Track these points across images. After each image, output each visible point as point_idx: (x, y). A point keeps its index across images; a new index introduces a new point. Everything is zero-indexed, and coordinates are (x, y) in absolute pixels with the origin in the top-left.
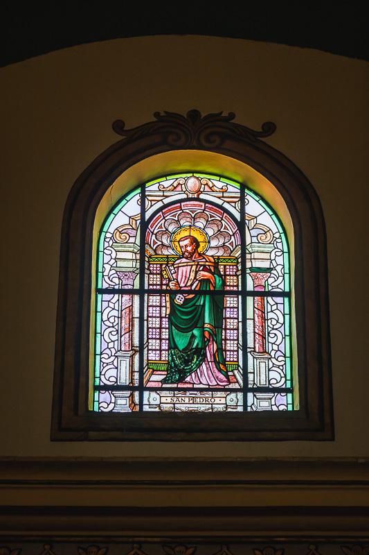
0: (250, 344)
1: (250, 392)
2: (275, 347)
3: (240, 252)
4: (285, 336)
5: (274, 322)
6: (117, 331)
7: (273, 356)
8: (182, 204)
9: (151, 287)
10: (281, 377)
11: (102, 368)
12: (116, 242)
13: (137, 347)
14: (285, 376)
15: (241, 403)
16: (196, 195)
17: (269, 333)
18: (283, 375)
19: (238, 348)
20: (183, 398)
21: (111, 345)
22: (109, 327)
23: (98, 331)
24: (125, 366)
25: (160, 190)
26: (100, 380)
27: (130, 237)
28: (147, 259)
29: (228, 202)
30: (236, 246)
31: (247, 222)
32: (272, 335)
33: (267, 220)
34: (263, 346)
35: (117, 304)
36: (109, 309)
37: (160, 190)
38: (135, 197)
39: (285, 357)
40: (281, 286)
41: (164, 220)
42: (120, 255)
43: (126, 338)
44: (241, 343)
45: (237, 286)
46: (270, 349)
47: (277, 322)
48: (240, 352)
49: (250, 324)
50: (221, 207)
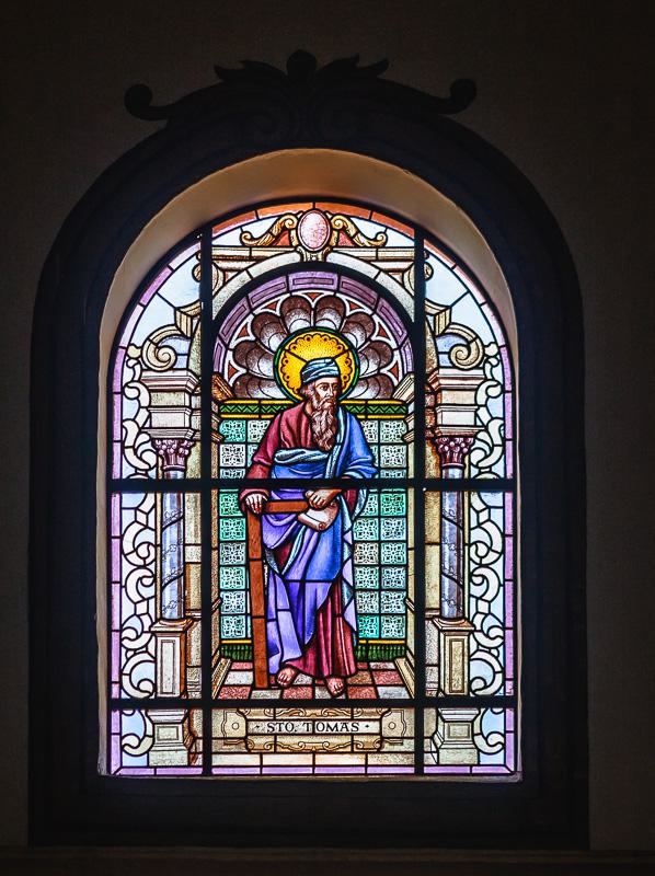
0: (432, 599)
1: (429, 706)
2: (483, 607)
3: (412, 389)
4: (505, 580)
5: (482, 550)
6: (154, 576)
7: (478, 628)
10: (495, 673)
11: (124, 660)
12: (149, 369)
13: (196, 610)
14: (503, 671)
15: (410, 732)
16: (320, 255)
17: (471, 574)
18: (498, 668)
19: (407, 607)
21: (142, 608)
22: (139, 567)
23: (116, 577)
24: (170, 652)
25: (244, 245)
26: (121, 687)
27: (177, 355)
28: (215, 408)
29: (387, 272)
30: (404, 376)
31: (430, 319)
32: (477, 580)
33: (471, 315)
34: (460, 605)
35: (152, 515)
36: (137, 527)
38: (187, 262)
39: (504, 628)
40: (499, 469)
43: (170, 594)
46: (473, 611)
47: (490, 549)
49: (432, 553)
50: (371, 283)
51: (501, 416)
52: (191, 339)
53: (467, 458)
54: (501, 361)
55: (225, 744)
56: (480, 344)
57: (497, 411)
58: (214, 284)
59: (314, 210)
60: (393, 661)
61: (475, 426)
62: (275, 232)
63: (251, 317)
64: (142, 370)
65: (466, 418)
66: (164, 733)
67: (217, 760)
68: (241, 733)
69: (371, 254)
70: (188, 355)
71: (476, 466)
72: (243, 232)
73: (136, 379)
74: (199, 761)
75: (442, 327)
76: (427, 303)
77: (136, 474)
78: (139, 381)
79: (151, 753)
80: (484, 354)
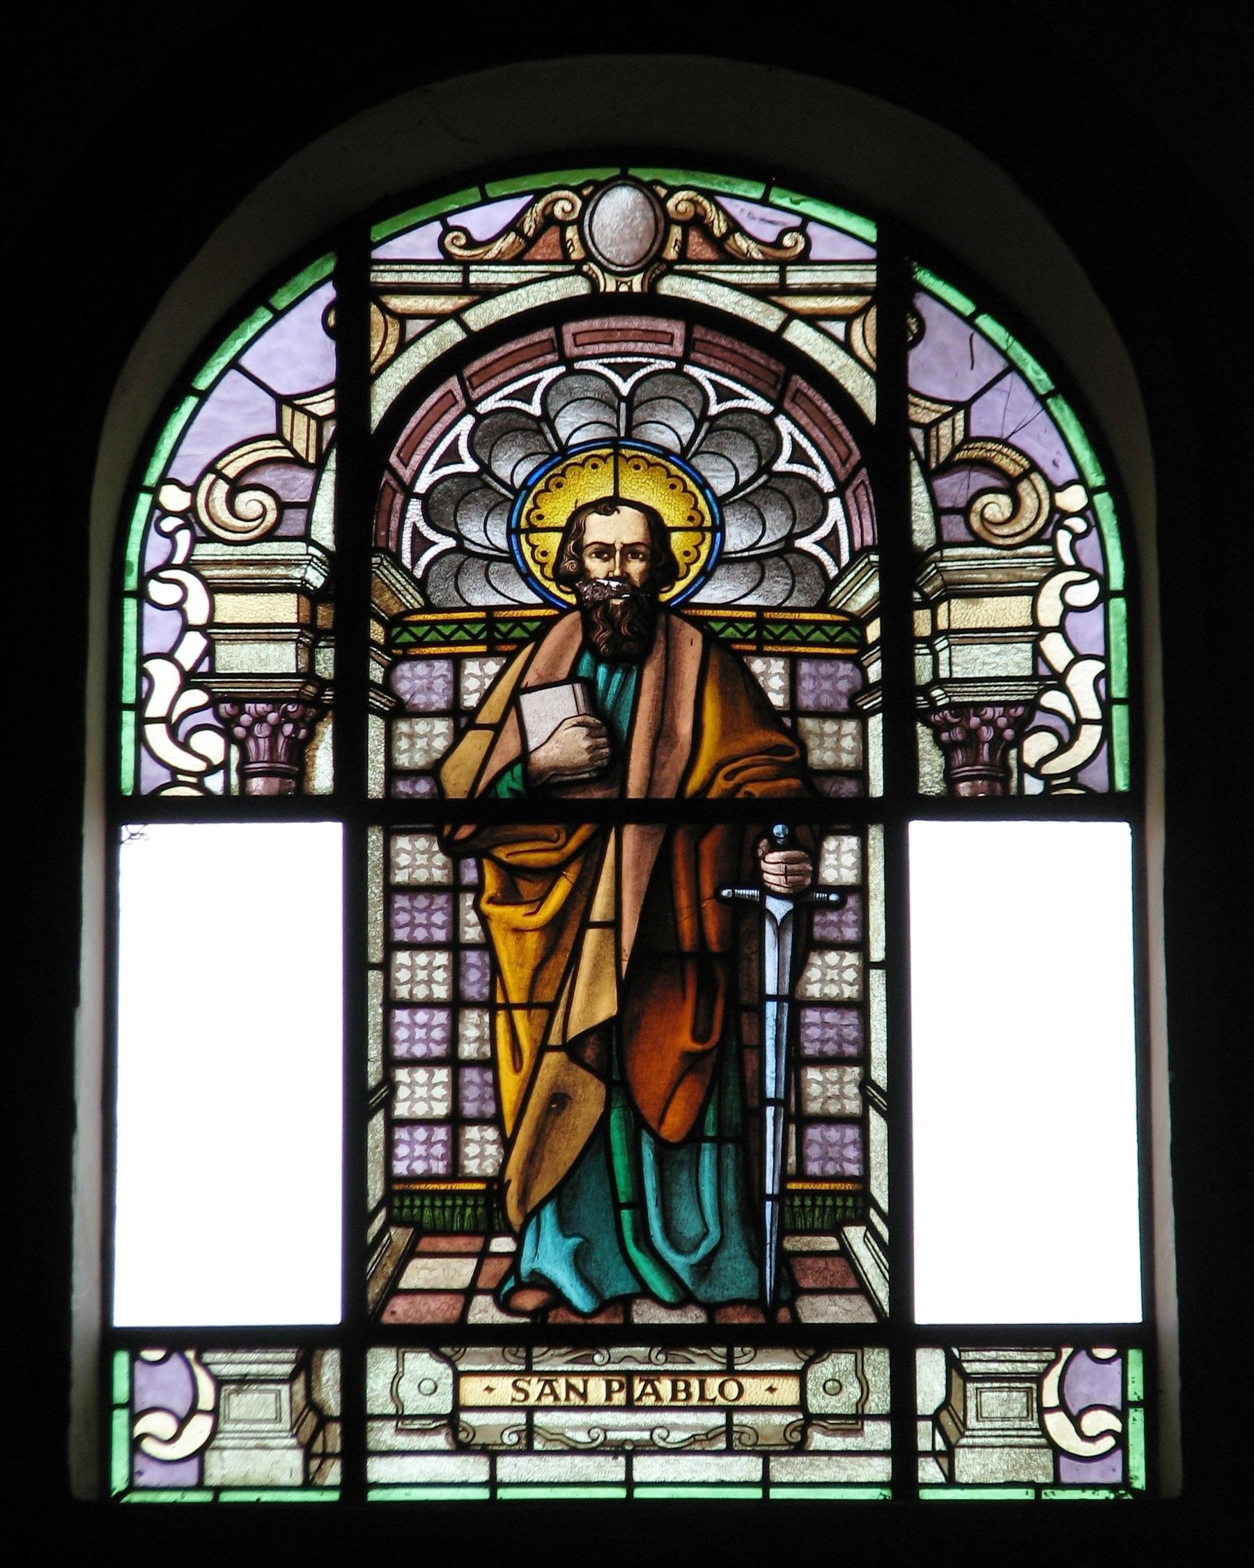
3: (874, 587)
8: (570, 328)
9: (403, 787)
12: (211, 538)
15: (880, 1401)
16: (637, 283)
19: (867, 1101)
20: (577, 1382)
25: (449, 259)
27: (282, 506)
28: (377, 632)
31: (917, 434)
37: (449, 259)
40: (1096, 778)
41: (468, 421)
42: (232, 608)
44: (879, 1074)
45: (860, 774)
48: (878, 1127)
50: (774, 343)
51: (1100, 651)
52: (319, 467)
53: (1013, 753)
54: (1094, 524)
55: (398, 1431)
56: (1042, 487)
57: (1089, 638)
58: (374, 352)
59: (624, 180)
60: (837, 1232)
61: (1035, 676)
62: (529, 226)
63: (468, 421)
64: (195, 540)
65: (1016, 659)
66: (241, 1405)
67: (377, 1470)
68: (443, 1404)
69: (769, 277)
70: (309, 506)
71: (1035, 772)
72: (447, 229)
73: (179, 559)
74: (334, 1473)
75: (945, 450)
76: (910, 397)
77: (175, 783)
78: (188, 566)
79: (207, 1454)
80: (1054, 509)
